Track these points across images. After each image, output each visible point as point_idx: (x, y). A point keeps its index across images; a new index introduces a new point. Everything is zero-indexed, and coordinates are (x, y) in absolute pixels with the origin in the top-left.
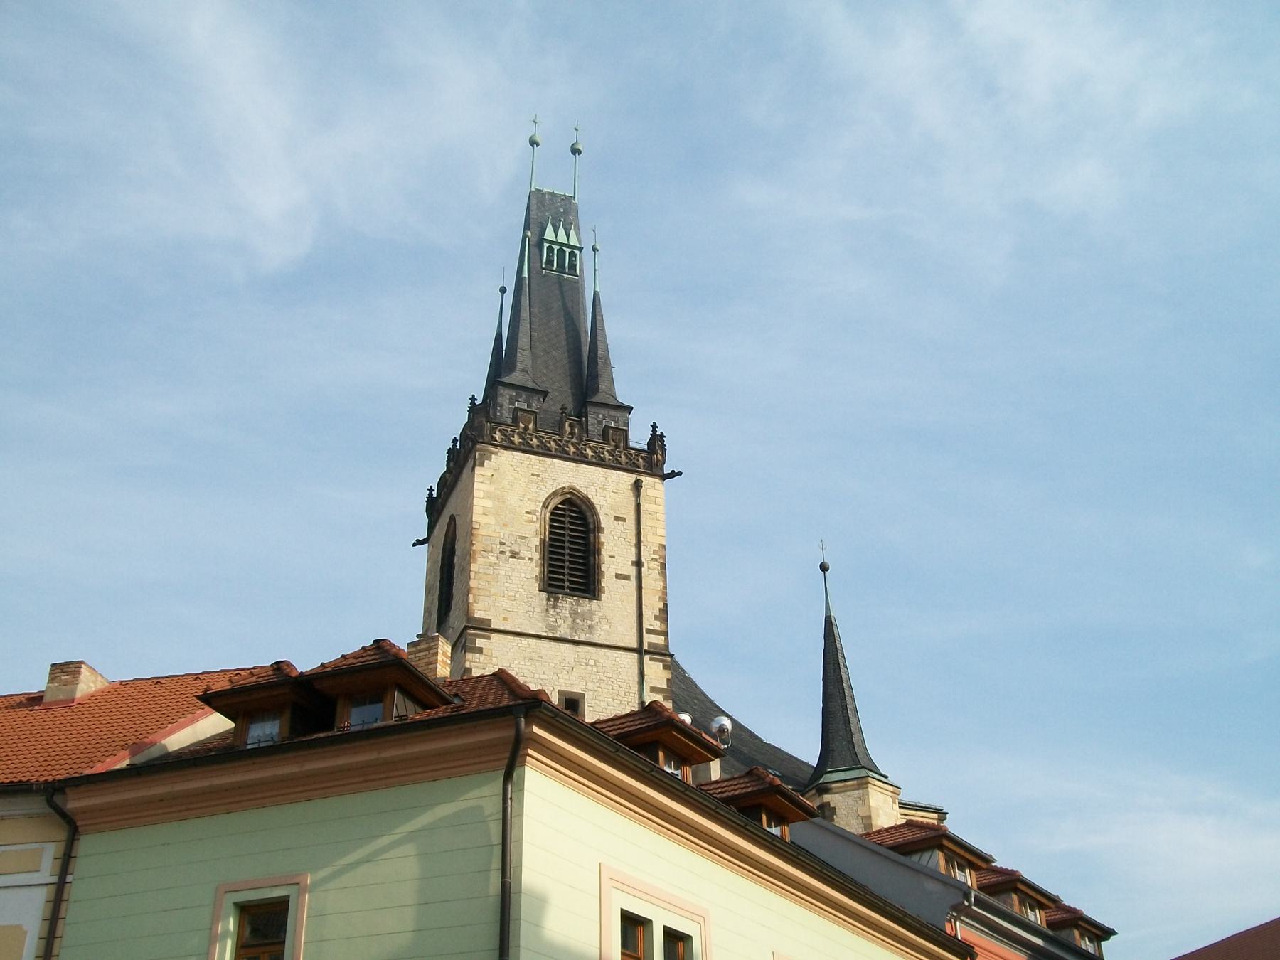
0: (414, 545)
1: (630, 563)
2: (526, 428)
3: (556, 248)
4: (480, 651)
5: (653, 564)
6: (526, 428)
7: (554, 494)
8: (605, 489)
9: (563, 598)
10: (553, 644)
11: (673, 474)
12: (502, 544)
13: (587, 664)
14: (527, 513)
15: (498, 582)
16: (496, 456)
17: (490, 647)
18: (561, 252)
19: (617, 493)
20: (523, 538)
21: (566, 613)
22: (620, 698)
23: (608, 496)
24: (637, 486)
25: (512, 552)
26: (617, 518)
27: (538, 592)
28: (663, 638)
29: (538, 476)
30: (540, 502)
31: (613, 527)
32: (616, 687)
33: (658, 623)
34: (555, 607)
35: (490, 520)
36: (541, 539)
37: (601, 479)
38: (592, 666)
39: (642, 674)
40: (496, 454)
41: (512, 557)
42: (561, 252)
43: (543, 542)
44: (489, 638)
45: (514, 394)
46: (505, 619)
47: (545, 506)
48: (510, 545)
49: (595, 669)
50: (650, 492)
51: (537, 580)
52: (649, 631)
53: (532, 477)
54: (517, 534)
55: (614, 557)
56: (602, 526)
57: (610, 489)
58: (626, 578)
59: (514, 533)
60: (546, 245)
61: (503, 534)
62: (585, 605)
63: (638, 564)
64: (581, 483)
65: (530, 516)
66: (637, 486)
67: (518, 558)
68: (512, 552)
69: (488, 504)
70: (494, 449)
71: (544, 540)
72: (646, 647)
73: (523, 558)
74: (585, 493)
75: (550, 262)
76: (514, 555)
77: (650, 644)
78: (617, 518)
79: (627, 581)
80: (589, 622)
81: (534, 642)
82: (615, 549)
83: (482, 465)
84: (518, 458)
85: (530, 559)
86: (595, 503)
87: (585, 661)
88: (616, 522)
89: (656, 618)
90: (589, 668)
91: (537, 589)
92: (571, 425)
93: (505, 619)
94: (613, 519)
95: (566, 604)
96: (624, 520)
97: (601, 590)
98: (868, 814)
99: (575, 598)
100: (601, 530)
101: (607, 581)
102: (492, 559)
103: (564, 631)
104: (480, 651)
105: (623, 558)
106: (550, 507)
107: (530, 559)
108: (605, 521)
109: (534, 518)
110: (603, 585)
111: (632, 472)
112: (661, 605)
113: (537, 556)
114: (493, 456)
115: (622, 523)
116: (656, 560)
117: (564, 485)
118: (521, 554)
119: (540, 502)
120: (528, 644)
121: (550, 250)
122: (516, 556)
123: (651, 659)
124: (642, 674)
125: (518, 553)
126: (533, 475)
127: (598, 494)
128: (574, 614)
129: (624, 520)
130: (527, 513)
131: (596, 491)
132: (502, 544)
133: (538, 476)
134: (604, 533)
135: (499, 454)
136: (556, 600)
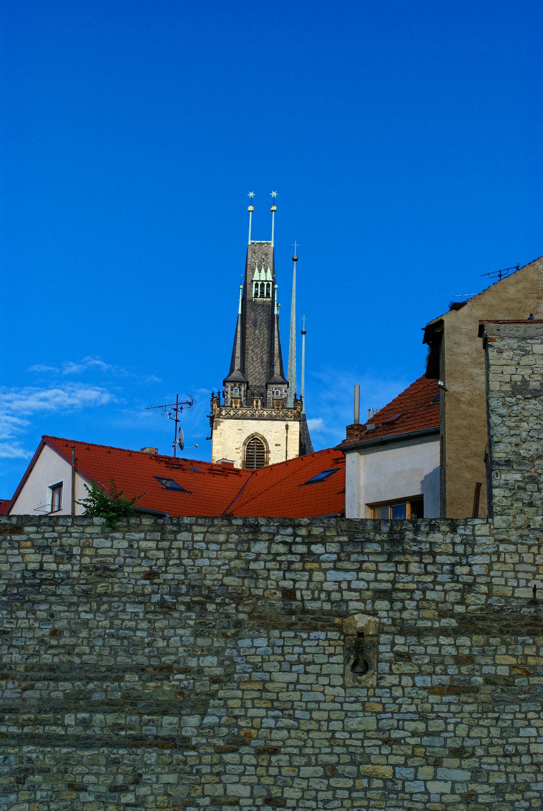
2: (236, 407)
3: (259, 283)
6: (236, 407)
18: (262, 285)
24: (287, 427)
26: (276, 445)
42: (262, 285)
47: (244, 444)
50: (292, 429)
57: (274, 431)
60: (254, 283)
66: (287, 427)
69: (219, 447)
70: (221, 420)
75: (256, 294)
78: (276, 445)
83: (216, 429)
92: (257, 402)
96: (279, 445)
100: (268, 452)
108: (272, 447)
109: (239, 451)
111: (285, 420)
121: (257, 285)
129: (279, 445)
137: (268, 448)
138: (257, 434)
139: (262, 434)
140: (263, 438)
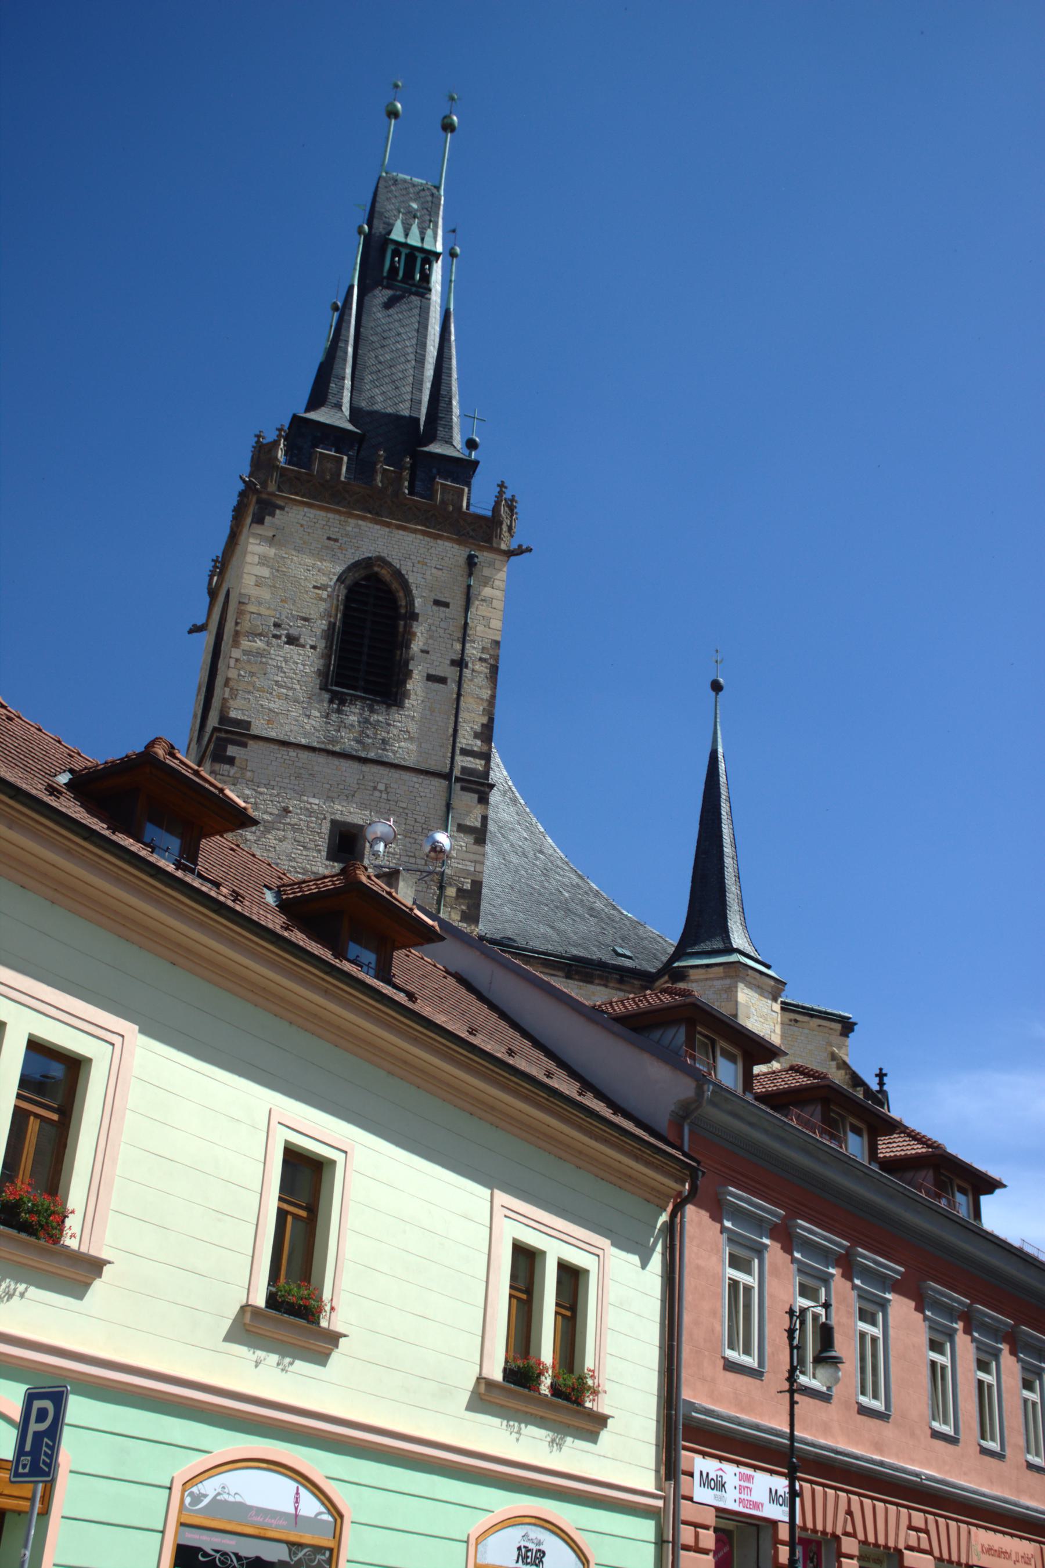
0: (190, 632)
1: (448, 662)
4: (231, 761)
5: (478, 667)
8: (425, 564)
9: (351, 700)
10: (336, 762)
11: (520, 551)
14: (315, 587)
15: (265, 674)
16: (282, 512)
17: (245, 757)
19: (441, 569)
20: (306, 619)
21: (353, 719)
22: (416, 836)
23: (428, 573)
25: (288, 636)
26: (437, 603)
27: (318, 691)
28: (483, 762)
29: (336, 540)
30: (334, 574)
31: (431, 614)
32: (411, 822)
33: (479, 743)
34: (339, 711)
35: (265, 594)
36: (330, 622)
37: (421, 551)
38: (381, 792)
40: (282, 508)
41: (287, 643)
43: (332, 626)
45: (319, 434)
48: (288, 627)
49: (384, 796)
52: (465, 752)
53: (328, 541)
56: (417, 611)
57: (433, 563)
58: (442, 680)
59: (294, 612)
63: (460, 663)
64: (393, 553)
65: (320, 592)
67: (297, 646)
68: (288, 636)
71: (335, 624)
72: (457, 772)
73: (303, 646)
74: (398, 567)
76: (292, 640)
77: (464, 769)
78: (437, 603)
79: (441, 685)
82: (430, 641)
84: (312, 516)
86: (410, 581)
87: (372, 784)
88: (435, 608)
89: (476, 736)
90: (377, 794)
91: (318, 686)
94: (432, 603)
96: (446, 605)
97: (405, 694)
98: (734, 1013)
99: (368, 702)
101: (416, 685)
102: (259, 644)
103: (347, 741)
104: (231, 761)
105: (439, 655)
106: (348, 582)
107: (313, 647)
109: (325, 594)
110: (408, 687)
112: (484, 720)
113: (321, 644)
114: (278, 512)
115: (444, 609)
117: (370, 555)
118: (302, 641)
119: (334, 574)
120: (297, 757)
123: (463, 789)
126: (329, 538)
127: (415, 569)
129: (446, 605)
130: (315, 587)
131: (414, 566)
133: (336, 540)
134: (417, 621)
135: (286, 509)
137: (411, 603)
138: (382, 561)
139: (396, 564)
140: (398, 574)
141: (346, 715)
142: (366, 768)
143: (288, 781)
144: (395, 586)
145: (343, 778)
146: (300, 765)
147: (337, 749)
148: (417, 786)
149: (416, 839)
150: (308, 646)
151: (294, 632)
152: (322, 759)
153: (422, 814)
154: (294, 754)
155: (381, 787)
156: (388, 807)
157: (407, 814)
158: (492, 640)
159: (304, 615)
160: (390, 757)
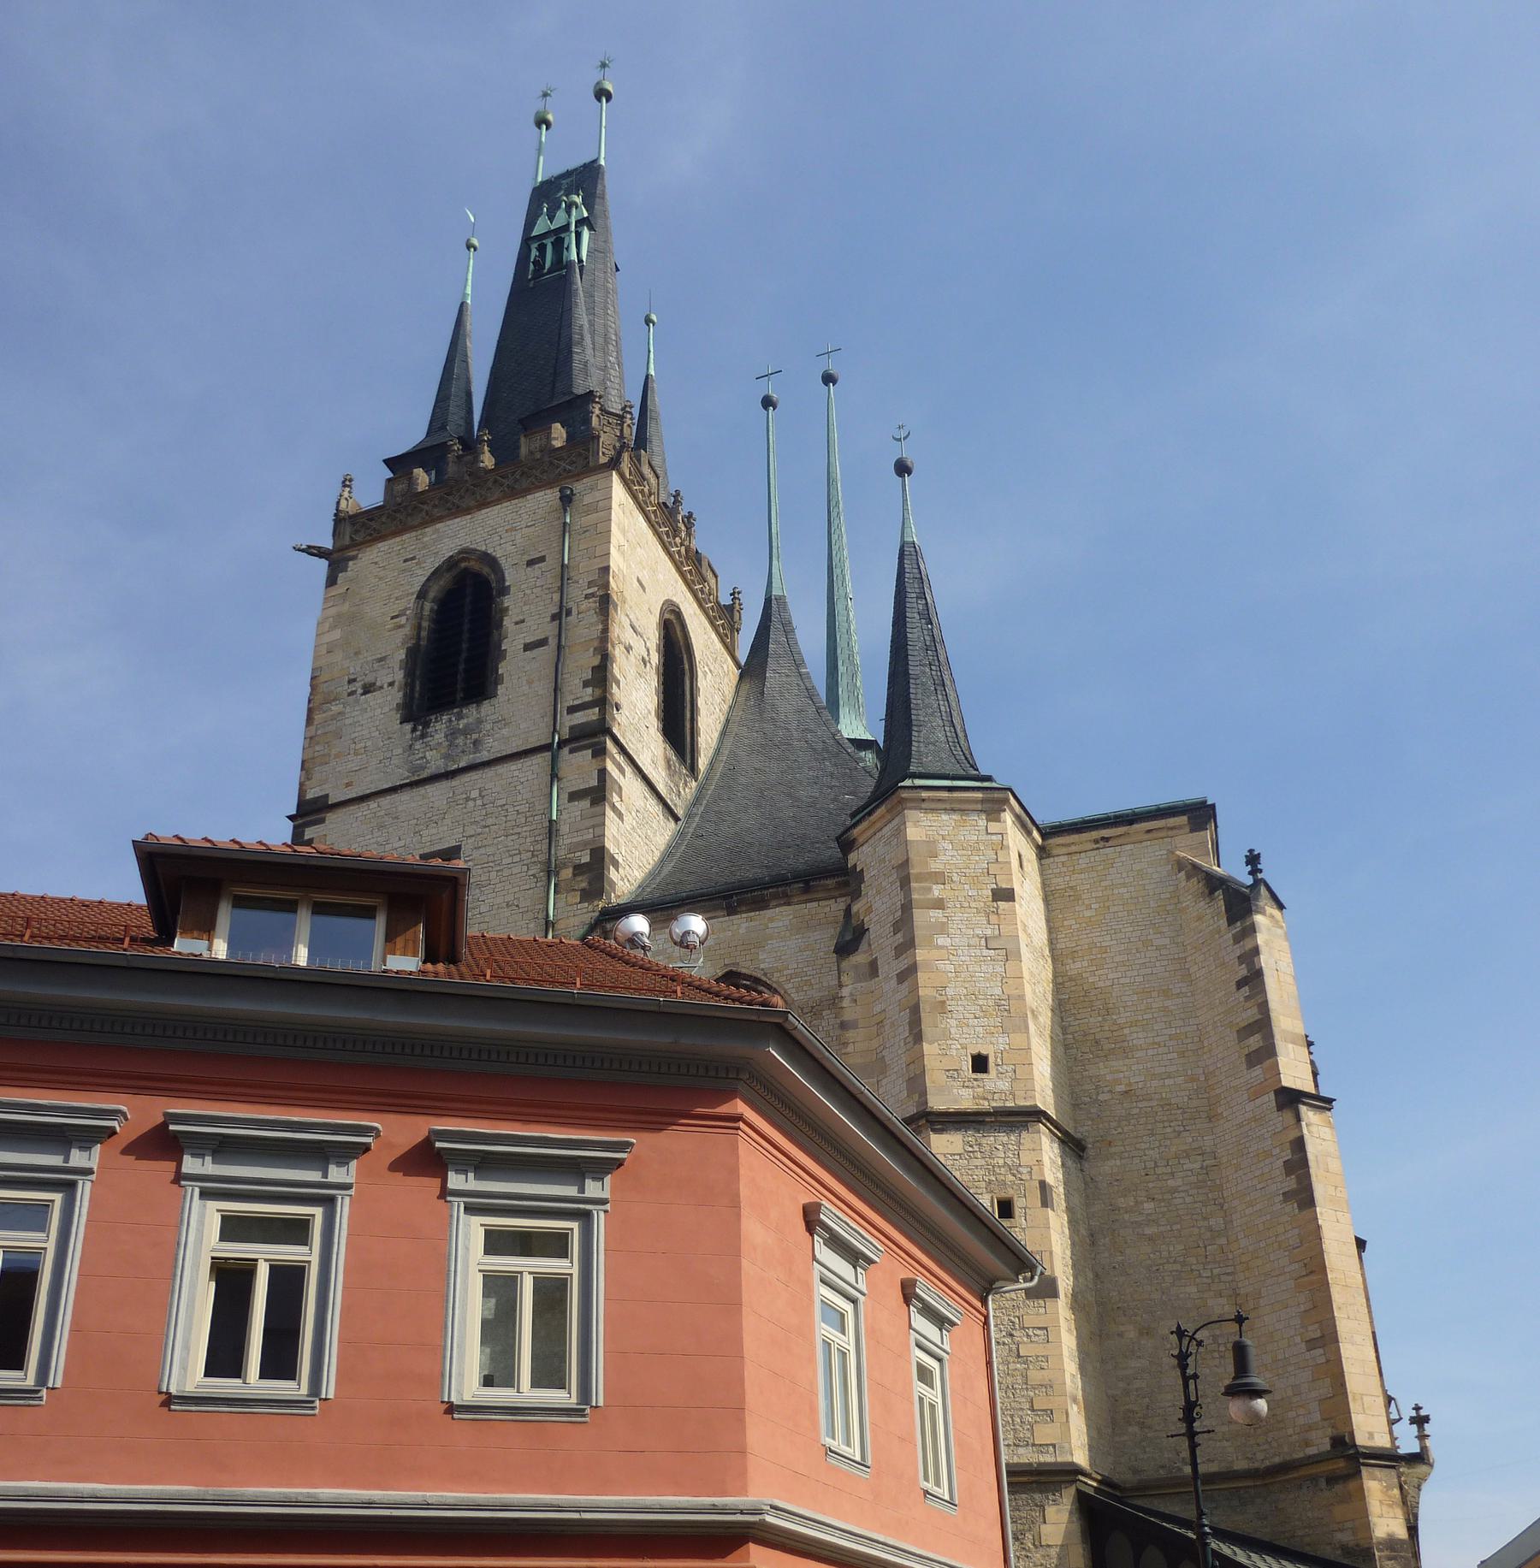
5: (585, 605)
7: (436, 574)
12: (351, 681)
13: (468, 799)
15: (341, 738)
22: (519, 830)
27: (399, 726)
38: (474, 800)
39: (554, 776)
41: (364, 693)
44: (322, 821)
46: (348, 785)
49: (479, 802)
51: (398, 710)
54: (374, 657)
55: (523, 621)
61: (354, 668)
62: (471, 713)
76: (368, 689)
78: (531, 563)
80: (475, 736)
81: (385, 801)
85: (391, 684)
87: (464, 796)
89: (586, 684)
90: (471, 804)
93: (348, 785)
95: (439, 728)
102: (335, 708)
116: (593, 595)
122: (372, 689)
123: (571, 751)
124: (554, 776)
125: (374, 684)
128: (452, 734)
132: (351, 681)
136: (426, 725)
141: (431, 736)
142: (455, 782)
143: (370, 836)
144: (486, 570)
145: (431, 805)
146: (382, 813)
147: (424, 775)
148: (517, 773)
149: (519, 833)
150: (385, 686)
151: (369, 679)
152: (404, 796)
153: (525, 802)
154: (376, 805)
155: (475, 794)
156: (484, 812)
157: (507, 810)
158: (599, 569)
159: (379, 656)
160: (485, 756)
